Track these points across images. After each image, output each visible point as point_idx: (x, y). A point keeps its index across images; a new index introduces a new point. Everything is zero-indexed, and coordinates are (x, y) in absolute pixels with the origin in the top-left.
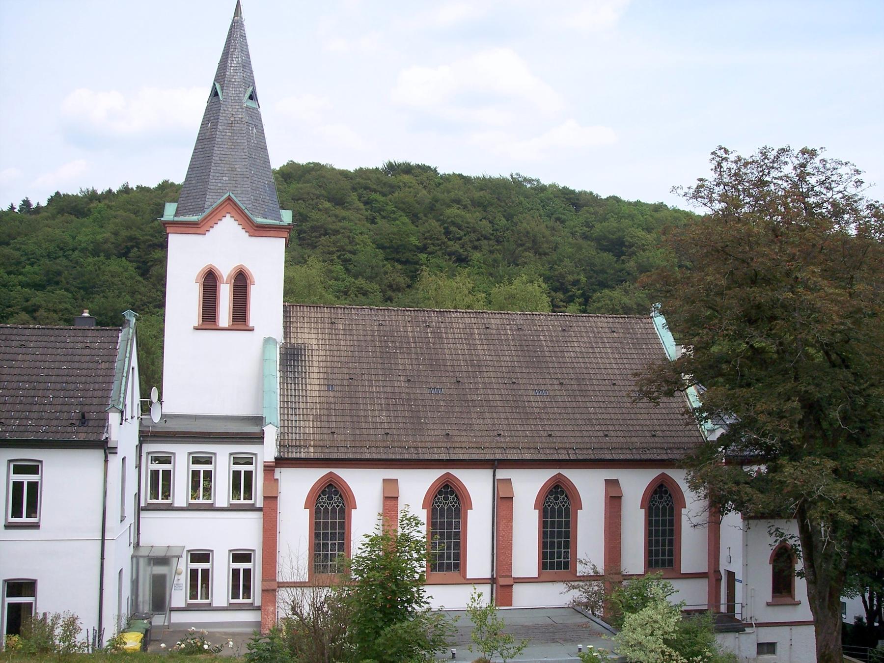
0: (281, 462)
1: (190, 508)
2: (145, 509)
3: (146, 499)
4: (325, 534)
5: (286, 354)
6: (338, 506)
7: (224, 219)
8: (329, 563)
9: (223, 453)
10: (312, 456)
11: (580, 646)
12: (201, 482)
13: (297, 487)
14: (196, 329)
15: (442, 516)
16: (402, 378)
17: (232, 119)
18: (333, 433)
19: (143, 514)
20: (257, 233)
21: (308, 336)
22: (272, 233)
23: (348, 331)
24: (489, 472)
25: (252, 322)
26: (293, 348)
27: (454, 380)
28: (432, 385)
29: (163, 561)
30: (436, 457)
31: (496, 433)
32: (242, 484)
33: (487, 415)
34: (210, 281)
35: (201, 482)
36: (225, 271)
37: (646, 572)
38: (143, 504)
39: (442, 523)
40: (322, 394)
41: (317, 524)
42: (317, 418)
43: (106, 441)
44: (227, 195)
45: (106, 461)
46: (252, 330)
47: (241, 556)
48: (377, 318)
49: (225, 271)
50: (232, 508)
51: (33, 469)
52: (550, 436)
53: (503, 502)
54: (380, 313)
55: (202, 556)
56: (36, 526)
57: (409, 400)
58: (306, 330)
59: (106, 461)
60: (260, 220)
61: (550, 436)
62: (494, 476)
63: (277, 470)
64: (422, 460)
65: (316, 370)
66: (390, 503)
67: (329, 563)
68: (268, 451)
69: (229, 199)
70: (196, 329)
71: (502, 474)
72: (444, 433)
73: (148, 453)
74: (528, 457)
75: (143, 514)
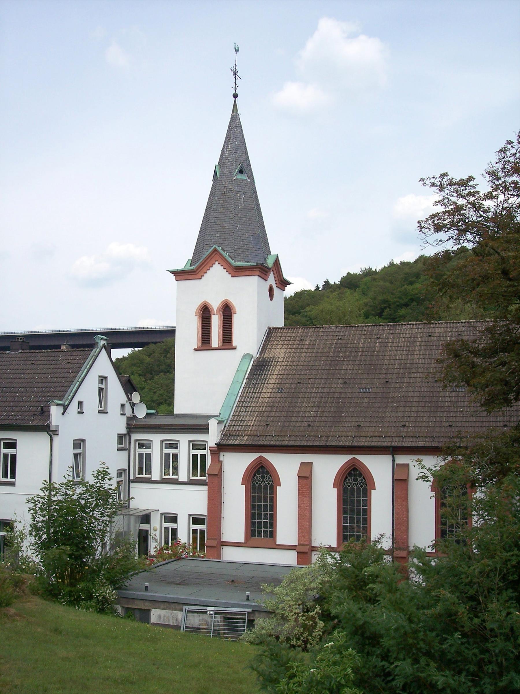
0: (221, 447)
1: (163, 481)
2: (133, 481)
3: (134, 474)
4: (260, 506)
5: (257, 366)
6: (269, 484)
7: (214, 266)
8: (263, 529)
9: (184, 440)
10: (244, 442)
11: (248, 593)
12: (171, 462)
13: (236, 467)
14: (196, 350)
15: (352, 494)
16: (340, 381)
17: (225, 190)
18: (267, 425)
19: (132, 485)
20: (236, 274)
21: (279, 352)
22: (247, 273)
23: (312, 346)
24: (389, 458)
25: (235, 343)
26: (264, 361)
27: (384, 381)
28: (363, 385)
29: (146, 518)
30: (341, 444)
31: (401, 424)
32: (197, 463)
33: (402, 409)
34: (205, 312)
35: (171, 462)
36: (215, 305)
37: (150, 513)
38: (132, 478)
39: (352, 501)
40: (275, 395)
41: (254, 498)
42: (261, 414)
43: (48, 426)
44: (214, 247)
45: (51, 440)
46: (235, 348)
47: (197, 520)
48: (339, 334)
49: (215, 305)
50: (191, 483)
51: (12, 445)
52: (450, 426)
53: (400, 484)
54: (343, 329)
55: (173, 519)
56: (13, 484)
57: (339, 398)
58: (279, 347)
59: (51, 440)
60: (239, 264)
61: (450, 426)
62: (394, 461)
63: (221, 454)
64: (327, 447)
65: (275, 377)
66: (304, 481)
67: (263, 529)
68: (212, 438)
69: (215, 250)
70: (196, 350)
71: (401, 459)
72: (357, 424)
73: (136, 441)
74: (421, 444)
75: (132, 485)
